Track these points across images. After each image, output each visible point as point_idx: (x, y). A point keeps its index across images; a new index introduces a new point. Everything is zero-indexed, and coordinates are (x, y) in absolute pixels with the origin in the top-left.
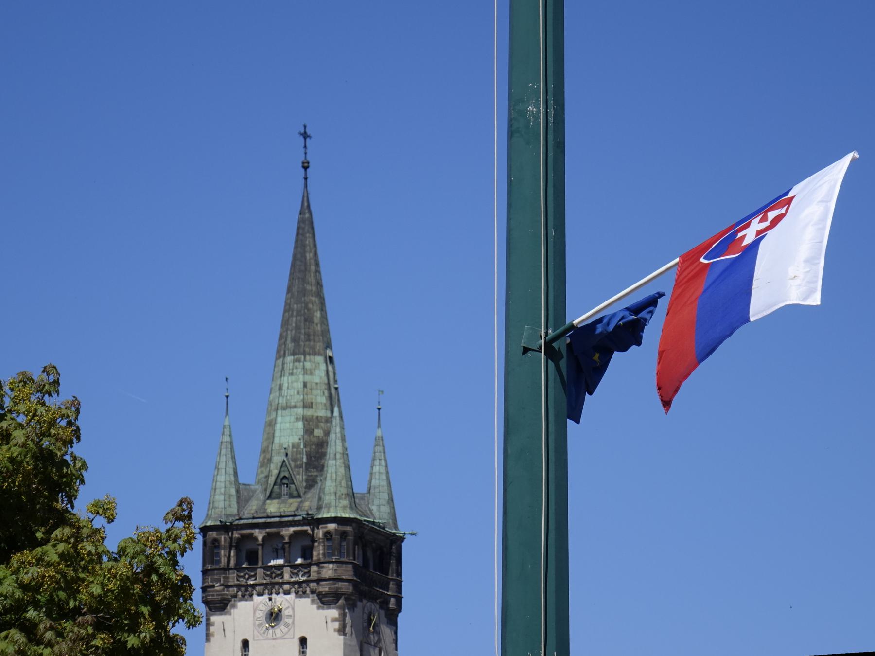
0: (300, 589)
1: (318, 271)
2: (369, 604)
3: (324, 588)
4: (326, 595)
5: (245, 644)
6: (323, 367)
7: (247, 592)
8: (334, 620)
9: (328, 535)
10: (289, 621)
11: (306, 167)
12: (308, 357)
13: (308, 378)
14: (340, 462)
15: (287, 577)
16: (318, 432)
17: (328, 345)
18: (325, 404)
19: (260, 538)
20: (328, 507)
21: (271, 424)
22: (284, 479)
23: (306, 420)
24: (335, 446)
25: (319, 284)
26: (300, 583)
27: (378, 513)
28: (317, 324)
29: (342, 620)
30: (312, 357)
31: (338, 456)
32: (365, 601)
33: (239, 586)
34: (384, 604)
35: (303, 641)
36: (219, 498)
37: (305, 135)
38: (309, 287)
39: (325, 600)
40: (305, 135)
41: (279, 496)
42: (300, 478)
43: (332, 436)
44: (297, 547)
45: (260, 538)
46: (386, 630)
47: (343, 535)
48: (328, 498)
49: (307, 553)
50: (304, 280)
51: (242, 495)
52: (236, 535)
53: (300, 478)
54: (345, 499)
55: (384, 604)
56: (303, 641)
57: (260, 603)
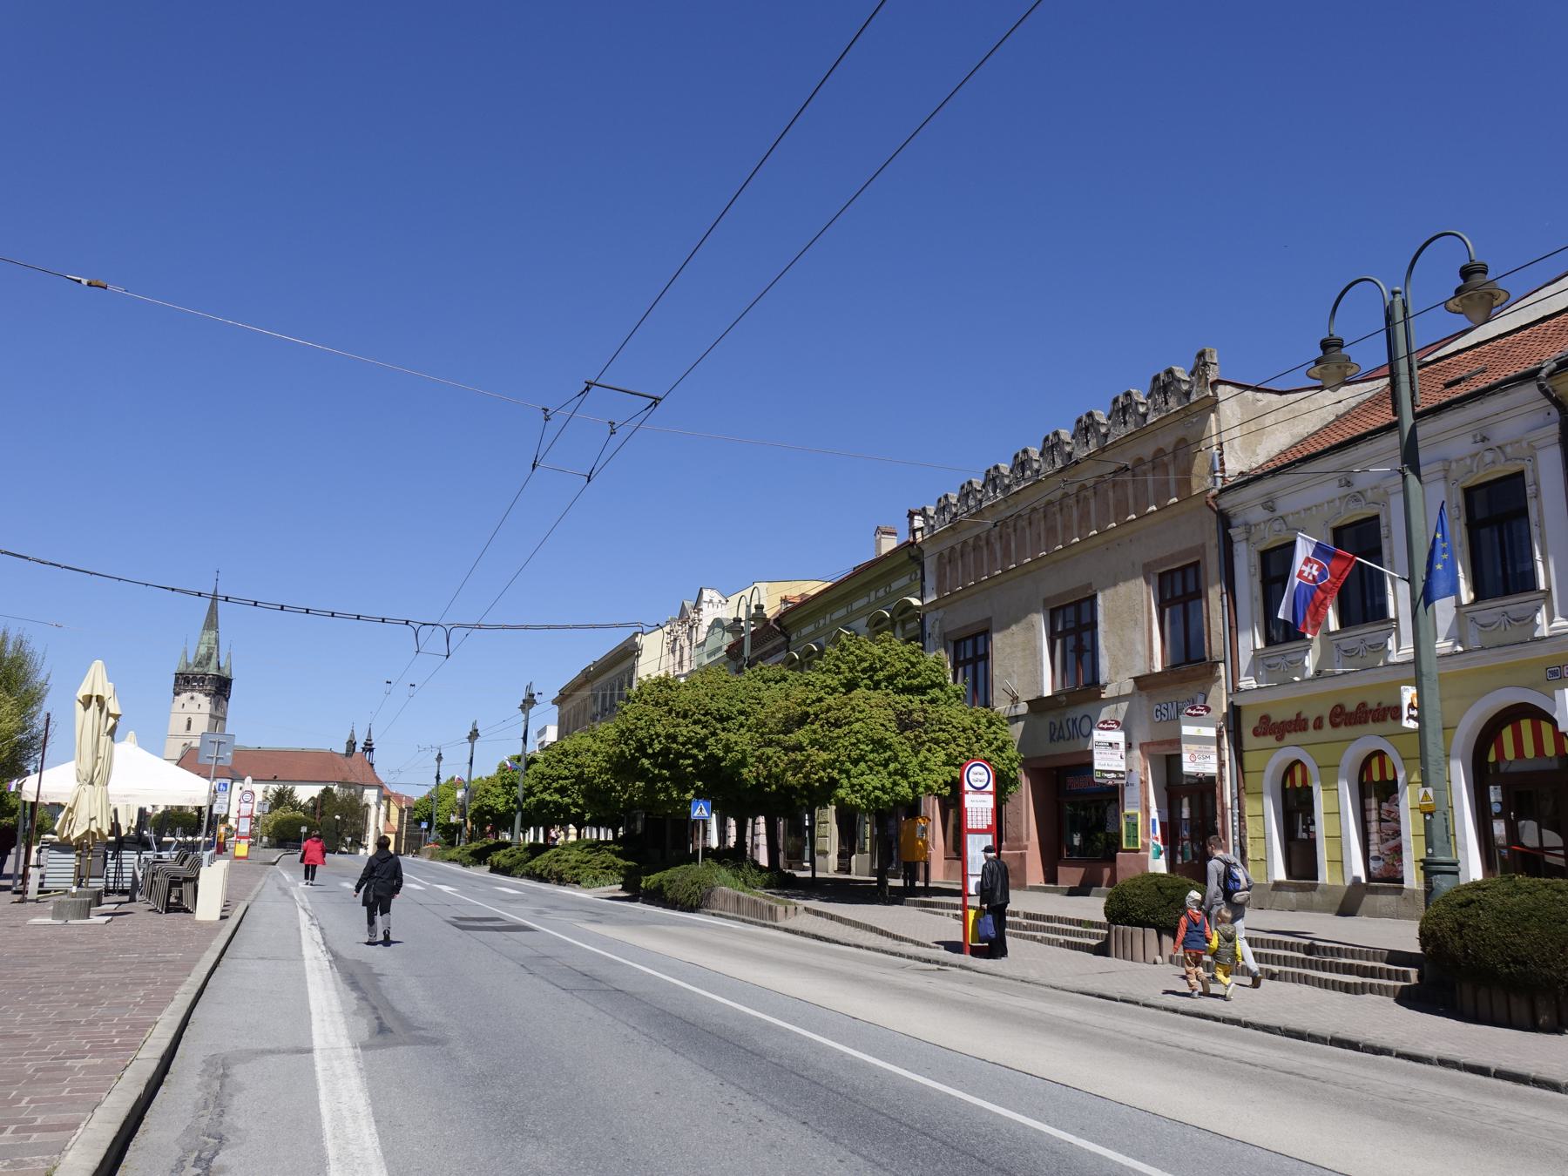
0: (200, 692)
7: (186, 691)
9: (209, 678)
17: (217, 628)
21: (198, 647)
24: (215, 655)
25: (217, 612)
27: (226, 673)
36: (181, 666)
39: (206, 695)
42: (204, 662)
46: (225, 703)
47: (213, 679)
48: (211, 669)
49: (203, 682)
51: (188, 665)
53: (204, 662)
55: (225, 696)
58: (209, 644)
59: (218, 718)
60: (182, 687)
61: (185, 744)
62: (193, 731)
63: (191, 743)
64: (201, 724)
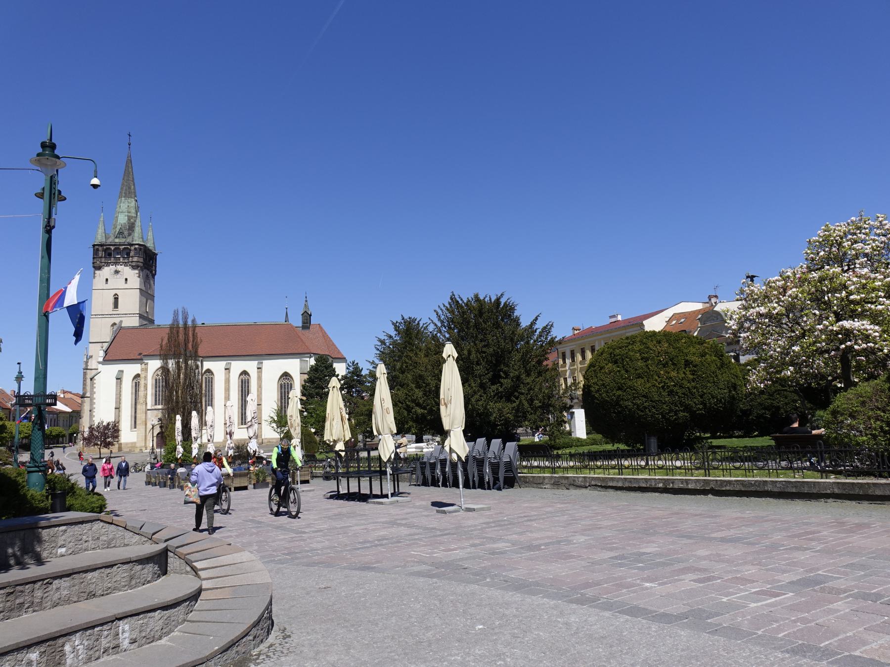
0: (126, 264)
1: (133, 175)
3: (134, 264)
4: (134, 266)
5: (107, 280)
6: (134, 202)
7: (108, 264)
8: (137, 274)
9: (135, 249)
14: (140, 228)
15: (121, 260)
16: (132, 220)
17: (136, 196)
19: (113, 249)
20: (136, 240)
22: (121, 233)
23: (128, 216)
24: (138, 223)
25: (133, 178)
26: (126, 263)
27: (150, 245)
29: (139, 274)
33: (105, 263)
34: (151, 272)
35: (126, 280)
37: (130, 135)
39: (134, 268)
40: (130, 135)
41: (119, 238)
42: (126, 233)
43: (137, 221)
44: (125, 252)
45: (113, 249)
47: (140, 249)
48: (135, 238)
49: (128, 254)
50: (128, 177)
52: (105, 247)
53: (126, 233)
56: (126, 280)
57: (112, 268)
58: (129, 212)
59: (147, 294)
60: (103, 260)
61: (114, 324)
62: (122, 308)
63: (121, 322)
64: (131, 302)
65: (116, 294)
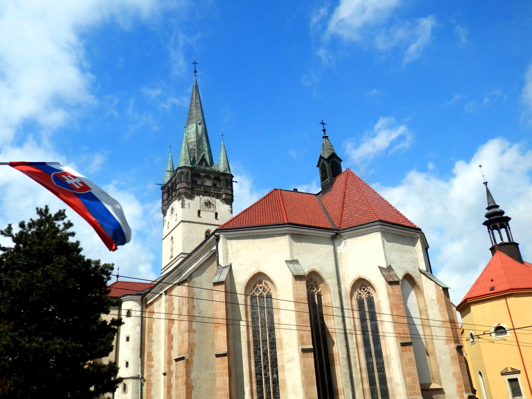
2: (206, 197)
6: (195, 126)
10: (174, 210)
11: (195, 72)
12: (190, 125)
13: (189, 131)
18: (194, 137)
28: (194, 114)
30: (191, 125)
31: (183, 148)
32: (201, 196)
37: (195, 63)
38: (192, 105)
54: (184, 161)
55: (218, 196)
56: (176, 214)
65: (172, 238)
